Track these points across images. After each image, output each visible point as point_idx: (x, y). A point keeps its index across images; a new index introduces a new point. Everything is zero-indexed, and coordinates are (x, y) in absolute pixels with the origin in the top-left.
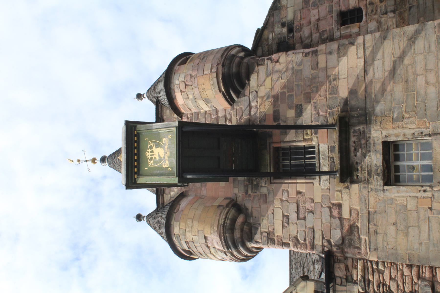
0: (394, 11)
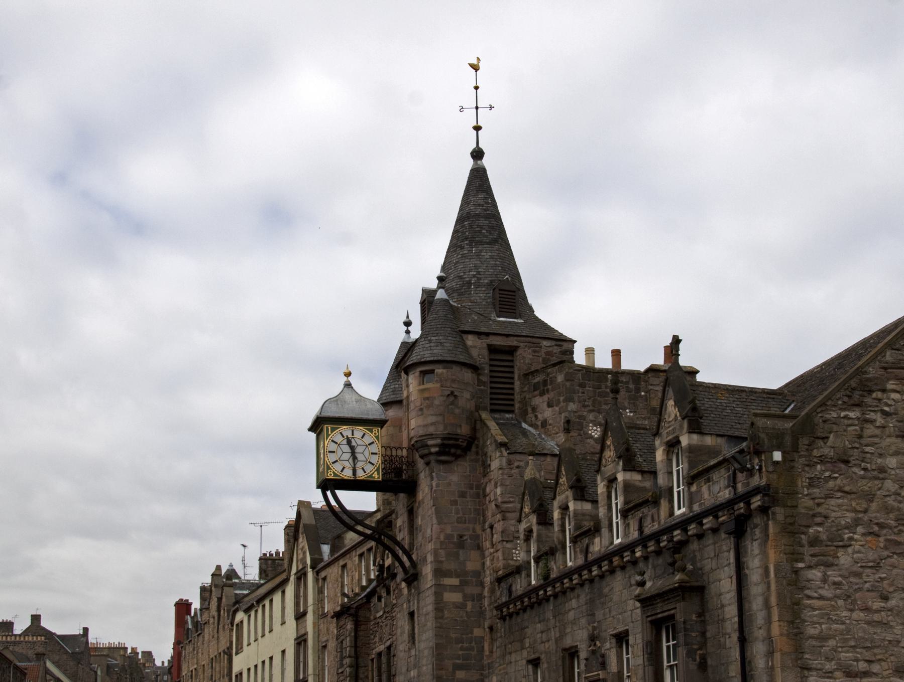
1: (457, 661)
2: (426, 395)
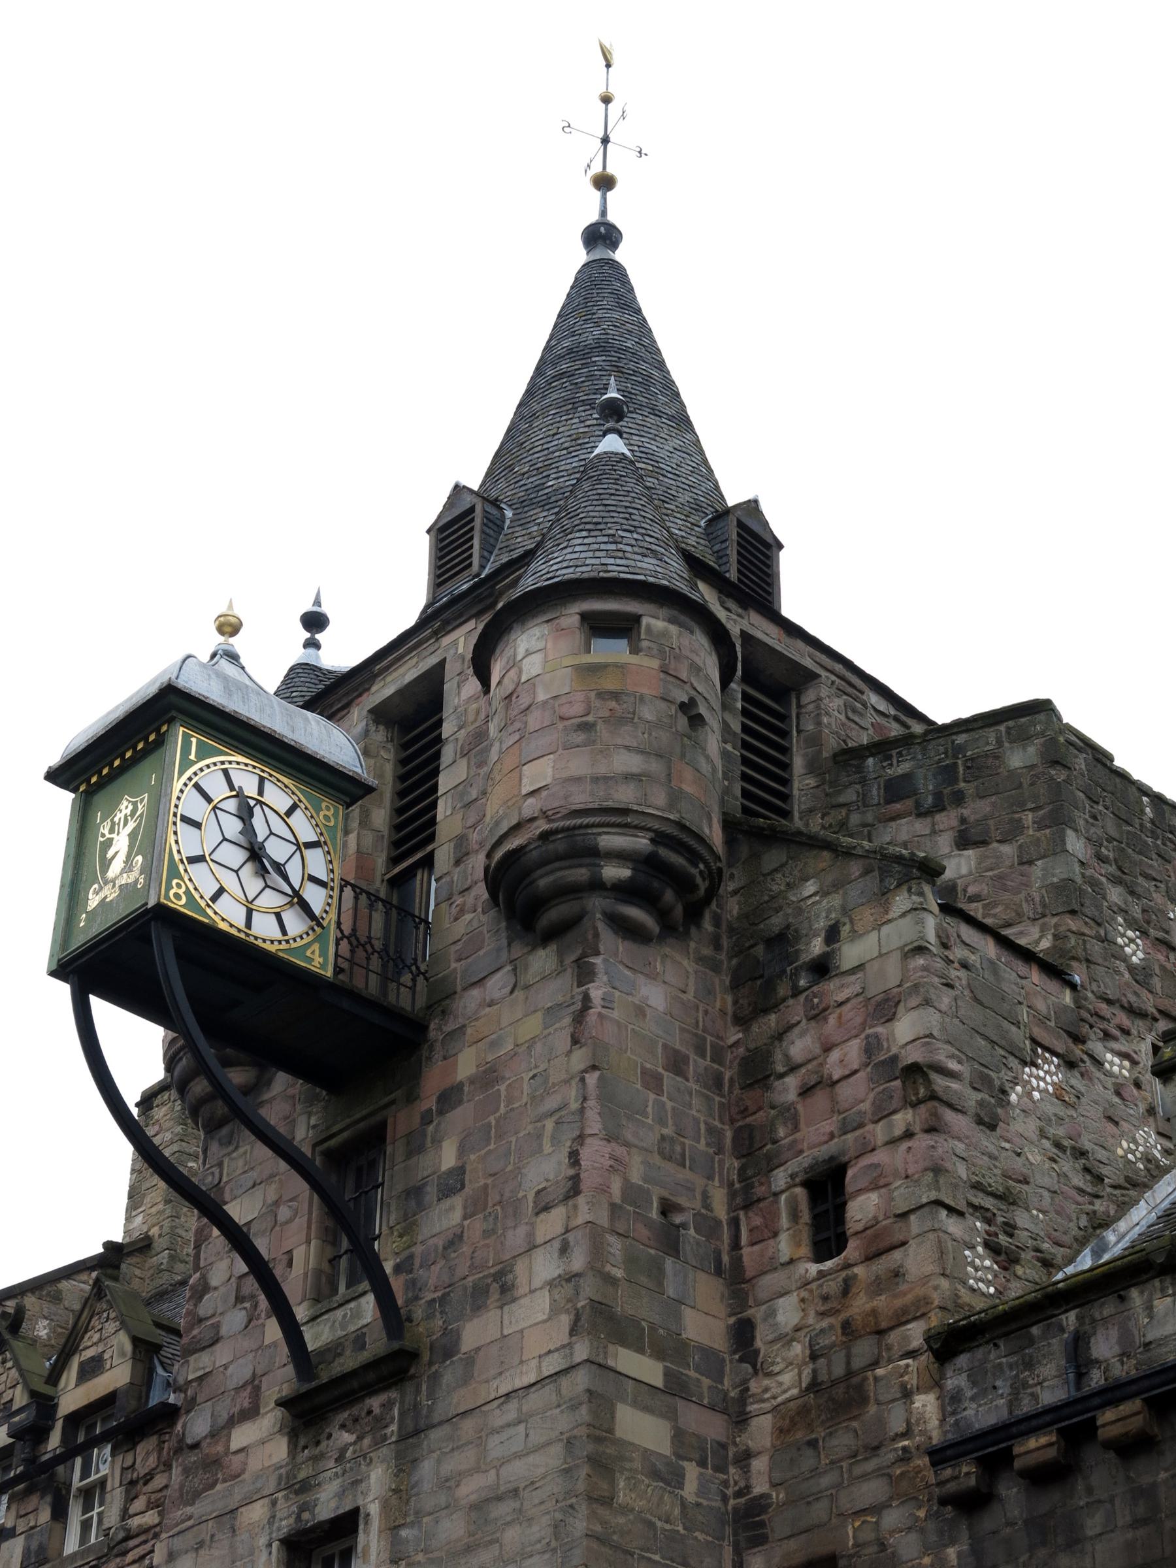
0: (814, 1386)
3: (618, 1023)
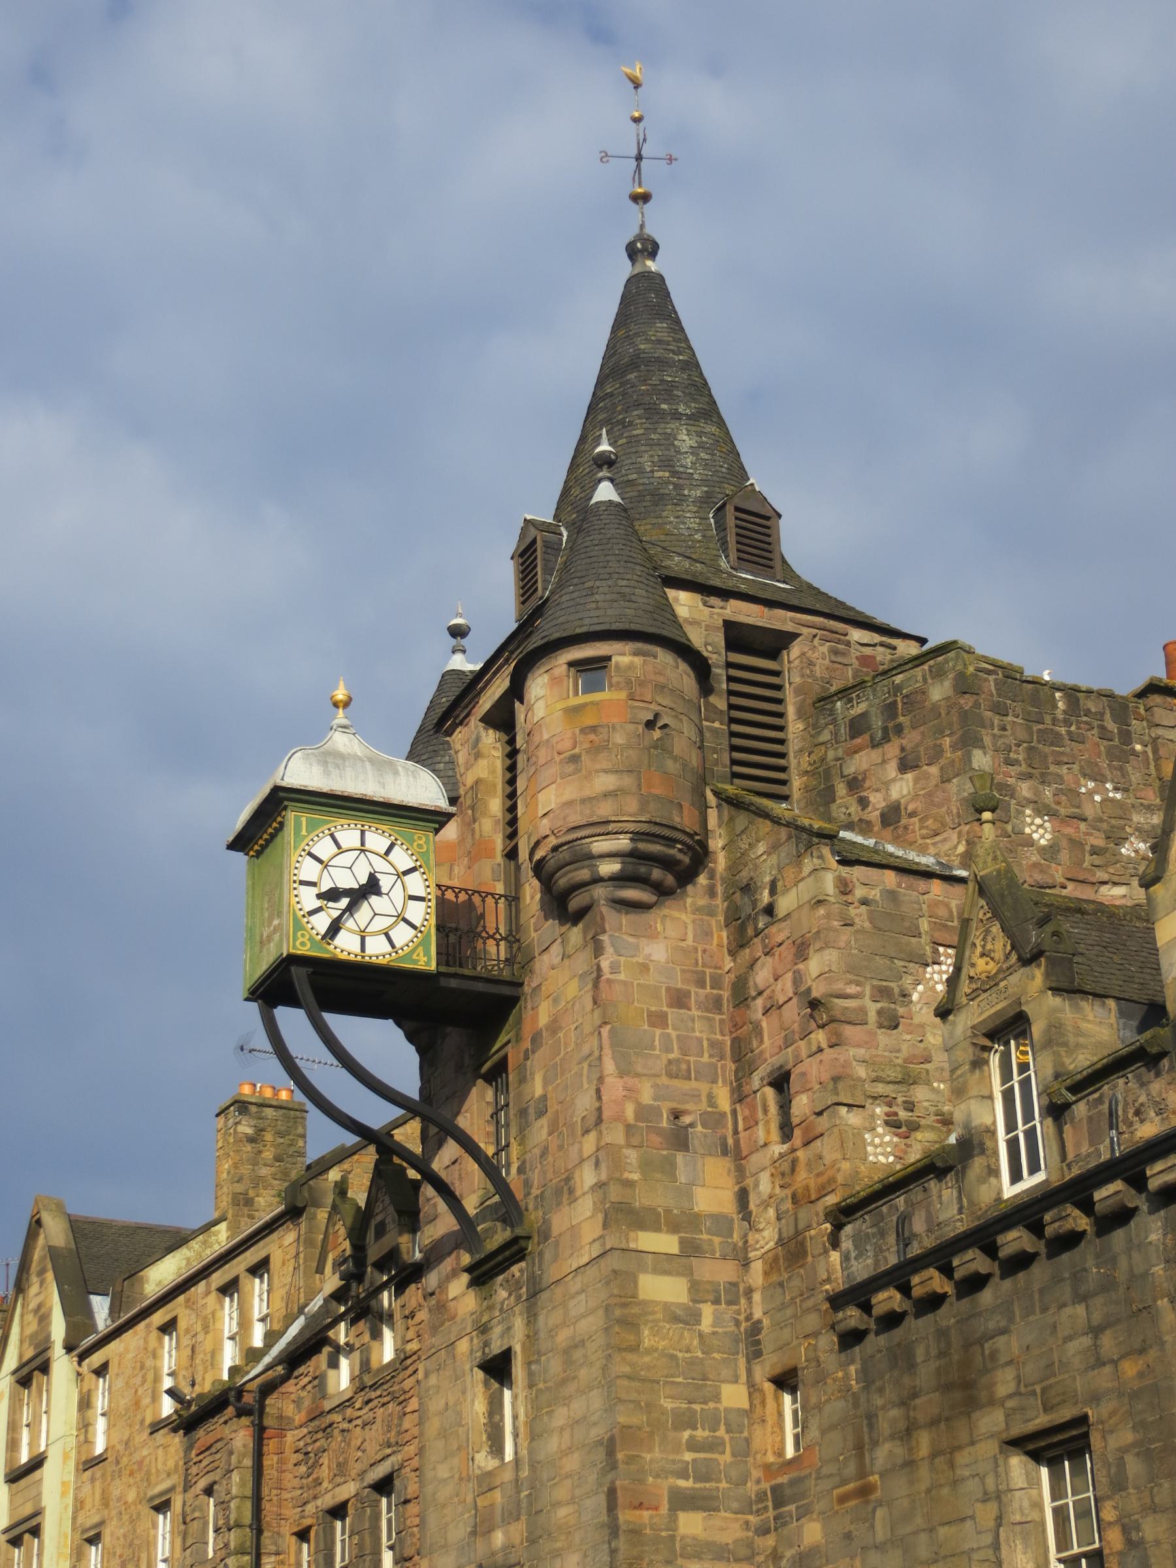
1: (682, 1483)
2: (589, 721)
3: (625, 983)
